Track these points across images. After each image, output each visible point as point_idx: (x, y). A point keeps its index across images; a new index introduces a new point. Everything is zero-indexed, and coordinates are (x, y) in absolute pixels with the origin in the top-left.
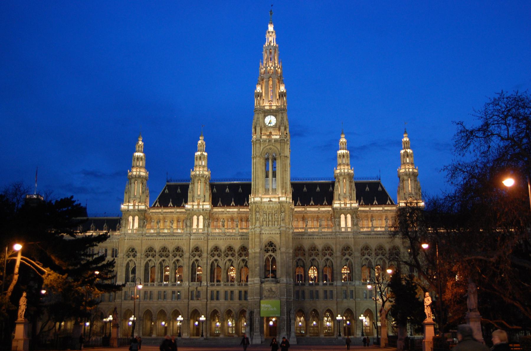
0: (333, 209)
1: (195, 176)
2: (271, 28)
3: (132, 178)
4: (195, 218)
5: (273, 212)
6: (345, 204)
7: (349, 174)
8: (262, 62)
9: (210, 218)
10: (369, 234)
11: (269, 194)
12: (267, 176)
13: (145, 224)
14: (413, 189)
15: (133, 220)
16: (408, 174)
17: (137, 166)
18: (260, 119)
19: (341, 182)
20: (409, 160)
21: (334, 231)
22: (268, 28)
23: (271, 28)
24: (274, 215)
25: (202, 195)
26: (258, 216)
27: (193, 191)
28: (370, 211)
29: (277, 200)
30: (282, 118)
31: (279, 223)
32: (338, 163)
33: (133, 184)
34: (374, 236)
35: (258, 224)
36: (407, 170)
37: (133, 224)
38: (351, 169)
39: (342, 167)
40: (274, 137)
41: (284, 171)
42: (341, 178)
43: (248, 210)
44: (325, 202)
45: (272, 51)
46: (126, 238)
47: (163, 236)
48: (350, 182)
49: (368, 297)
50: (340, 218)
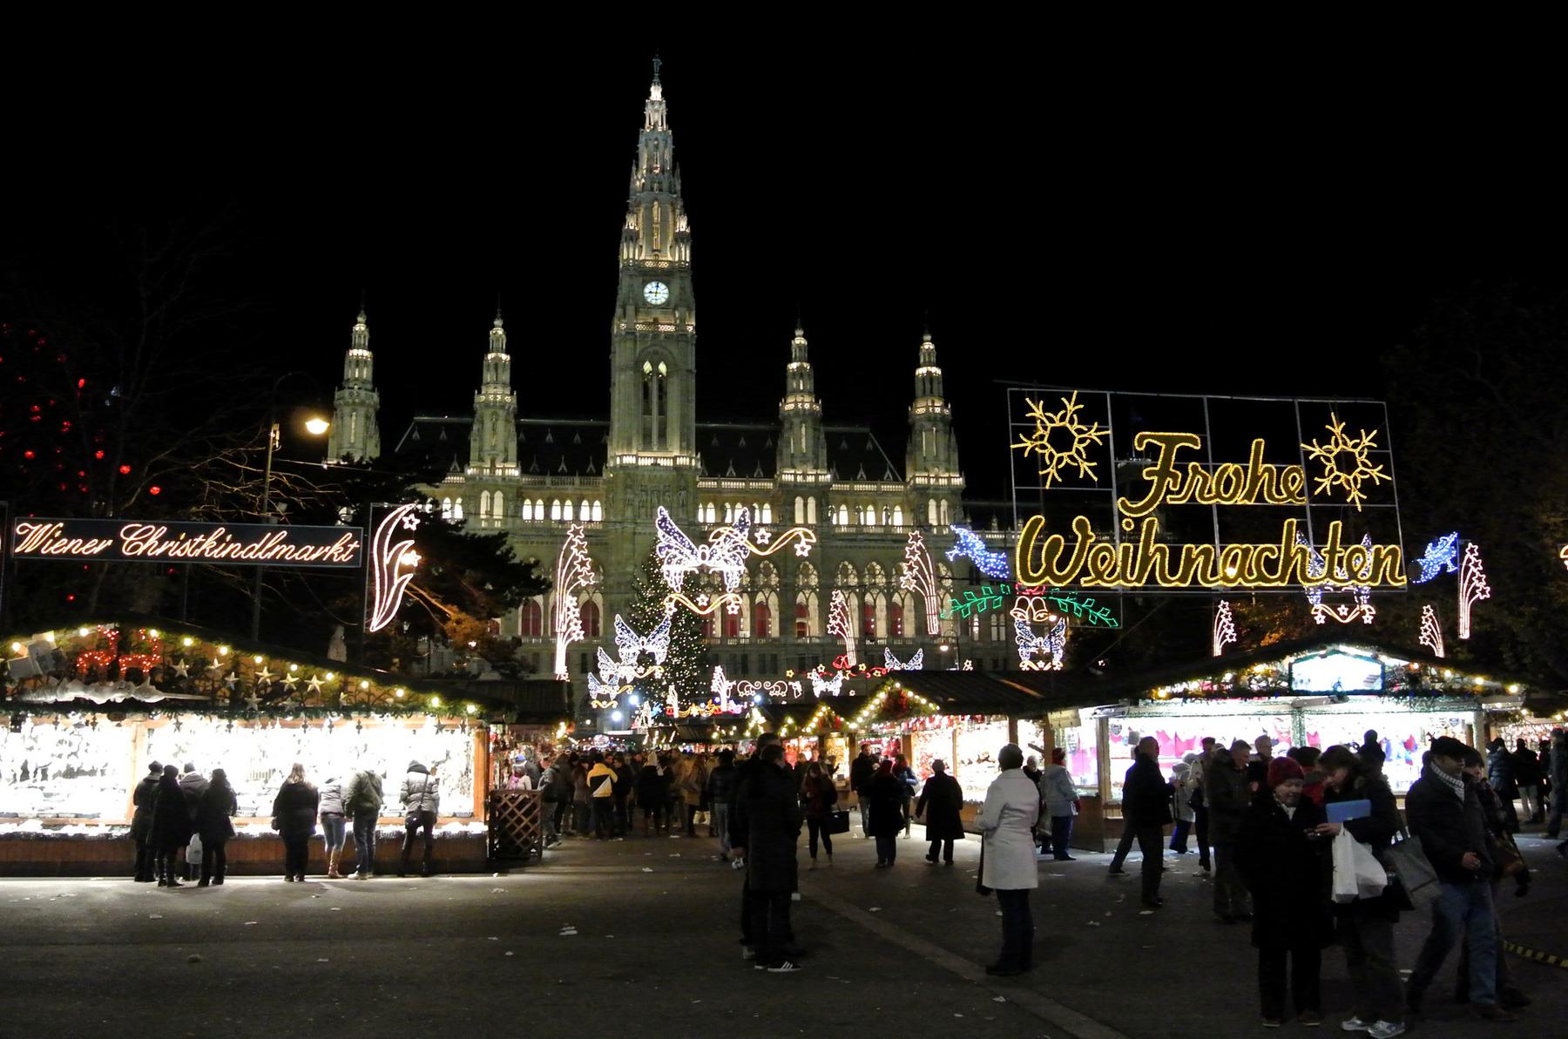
1: (487, 405)
2: (656, 93)
6: (805, 475)
7: (812, 412)
9: (516, 496)
11: (651, 450)
12: (647, 411)
14: (942, 449)
16: (931, 418)
19: (796, 428)
23: (656, 93)
25: (501, 447)
26: (630, 496)
27: (481, 439)
28: (852, 492)
29: (670, 463)
30: (682, 289)
33: (346, 419)
35: (629, 513)
39: (799, 399)
40: (663, 328)
41: (684, 404)
42: (796, 421)
45: (662, 144)
50: (793, 504)
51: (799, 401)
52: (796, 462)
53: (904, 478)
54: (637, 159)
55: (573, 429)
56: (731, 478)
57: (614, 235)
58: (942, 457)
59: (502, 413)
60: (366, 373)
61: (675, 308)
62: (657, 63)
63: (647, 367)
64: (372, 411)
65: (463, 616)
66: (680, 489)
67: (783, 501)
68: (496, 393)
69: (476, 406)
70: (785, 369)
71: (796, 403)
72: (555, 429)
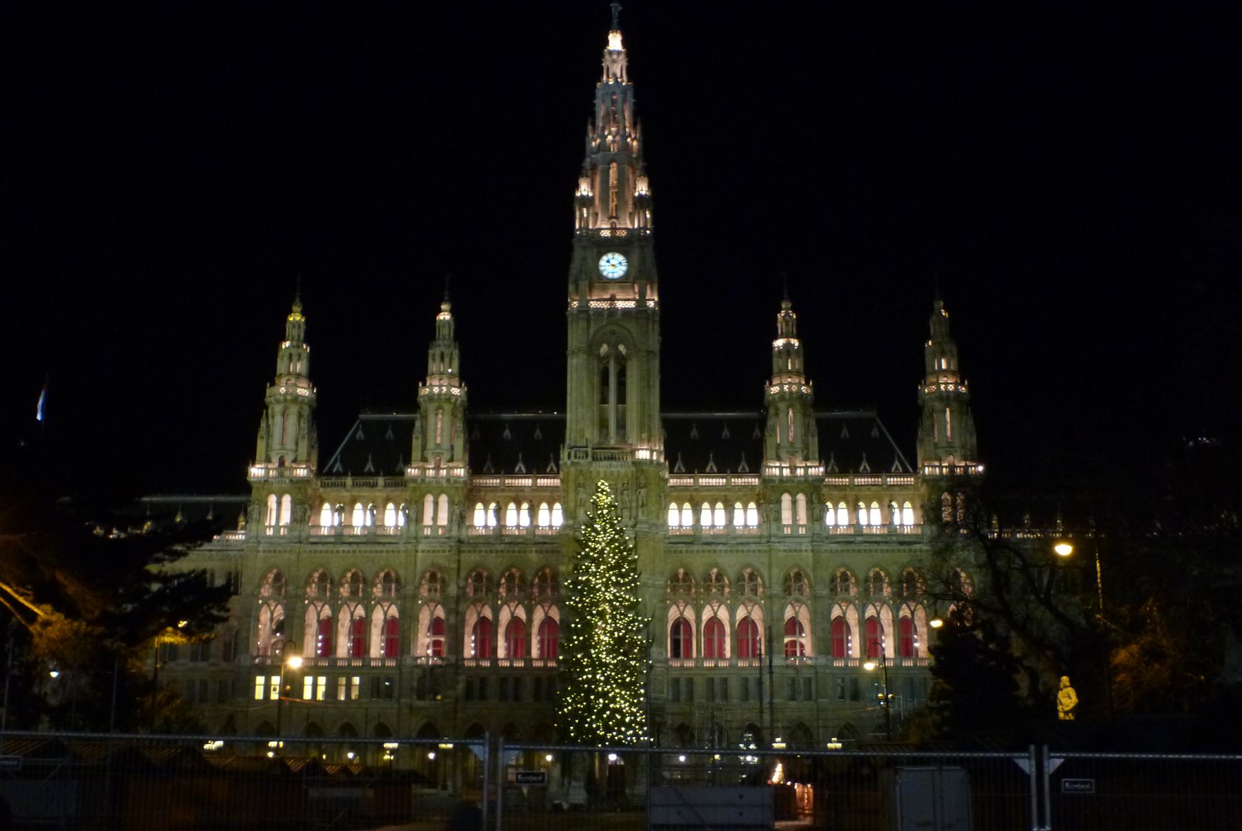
0: (766, 481)
1: (431, 398)
2: (615, 42)
3: (278, 401)
4: (429, 499)
5: (620, 485)
6: (793, 468)
7: (801, 396)
8: (594, 125)
10: (850, 543)
12: (604, 400)
13: (309, 513)
15: (279, 504)
16: (945, 398)
17: (289, 374)
18: (590, 261)
19: (782, 415)
20: (948, 364)
21: (765, 533)
22: (607, 43)
23: (615, 42)
24: (622, 494)
25: (446, 445)
28: (852, 486)
30: (643, 260)
31: (634, 513)
32: (775, 369)
33: (278, 419)
34: (863, 547)
36: (942, 387)
37: (278, 514)
38: (807, 384)
40: (620, 305)
42: (782, 406)
43: (557, 482)
44: (744, 464)
46: (261, 548)
47: (351, 543)
48: (805, 415)
49: (847, 695)
50: (779, 502)
51: (786, 385)
52: (783, 454)
53: (915, 468)
54: (593, 114)
55: (532, 423)
56: (711, 474)
57: (567, 203)
58: (957, 443)
59: (447, 407)
60: (301, 367)
61: (633, 283)
62: (616, 8)
63: (604, 349)
64: (306, 411)
65: (57, 617)
66: (639, 486)
67: (767, 498)
68: (443, 385)
69: (420, 400)
70: (771, 348)
71: (781, 385)
72: (514, 424)
